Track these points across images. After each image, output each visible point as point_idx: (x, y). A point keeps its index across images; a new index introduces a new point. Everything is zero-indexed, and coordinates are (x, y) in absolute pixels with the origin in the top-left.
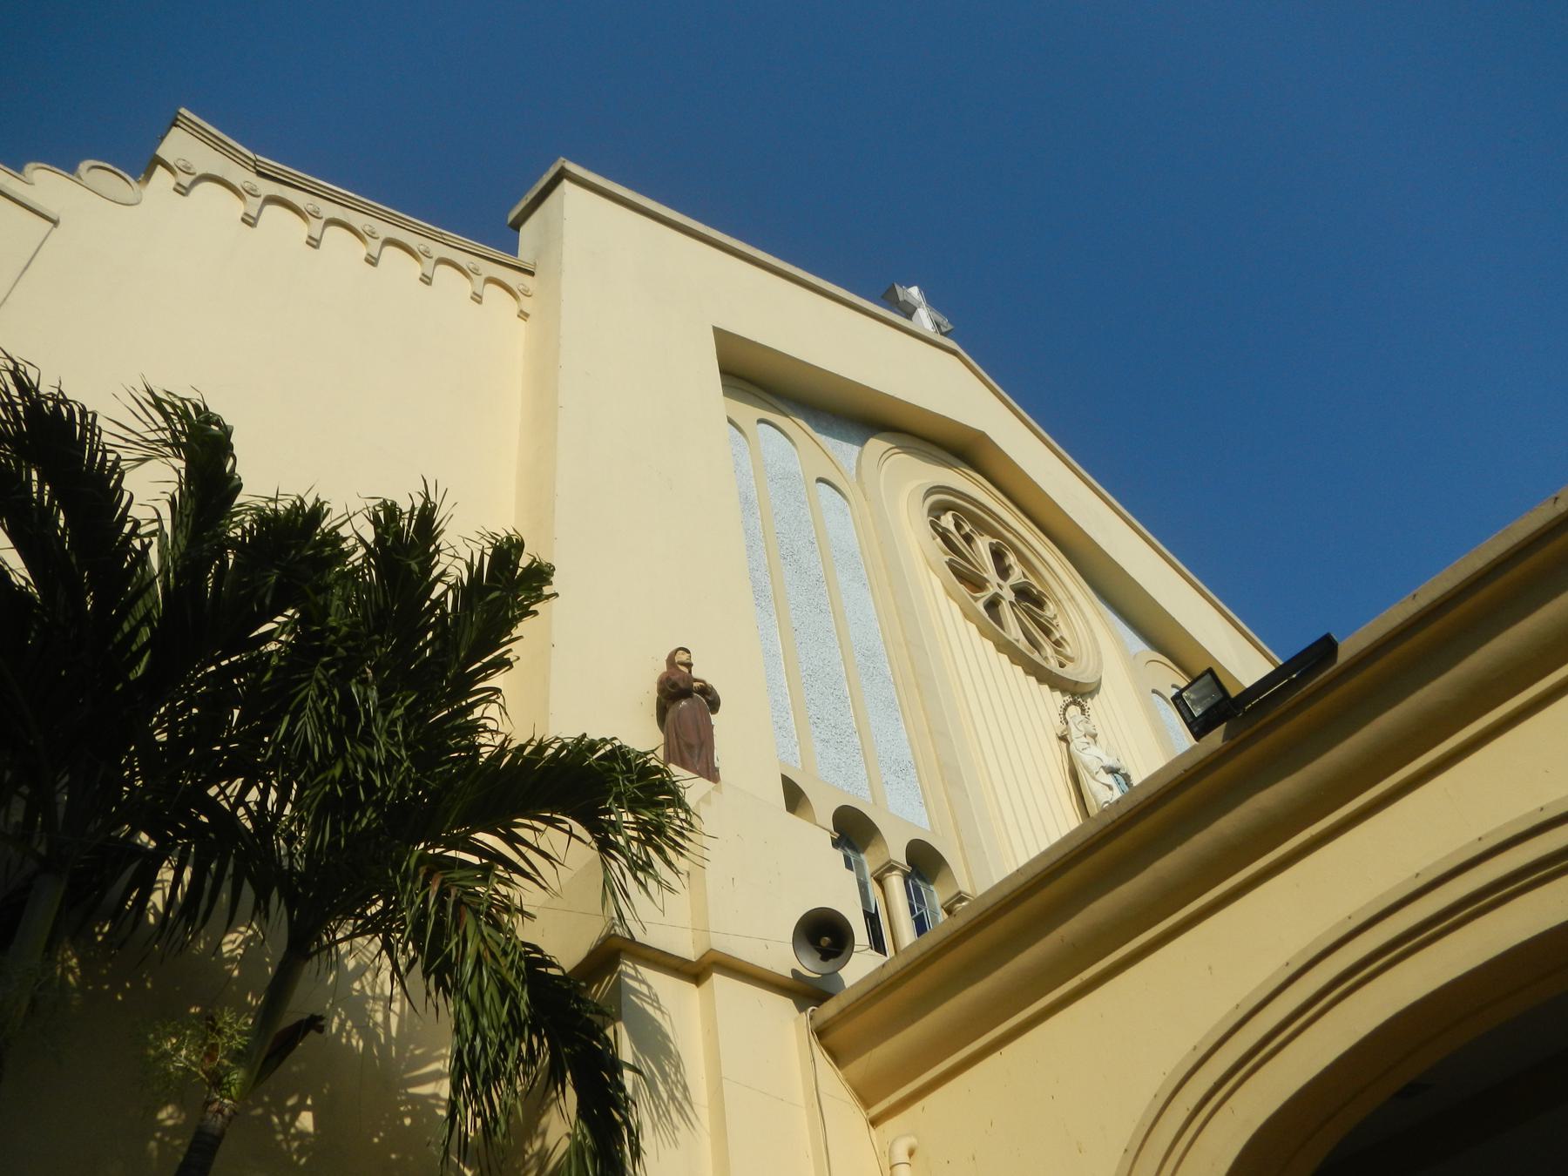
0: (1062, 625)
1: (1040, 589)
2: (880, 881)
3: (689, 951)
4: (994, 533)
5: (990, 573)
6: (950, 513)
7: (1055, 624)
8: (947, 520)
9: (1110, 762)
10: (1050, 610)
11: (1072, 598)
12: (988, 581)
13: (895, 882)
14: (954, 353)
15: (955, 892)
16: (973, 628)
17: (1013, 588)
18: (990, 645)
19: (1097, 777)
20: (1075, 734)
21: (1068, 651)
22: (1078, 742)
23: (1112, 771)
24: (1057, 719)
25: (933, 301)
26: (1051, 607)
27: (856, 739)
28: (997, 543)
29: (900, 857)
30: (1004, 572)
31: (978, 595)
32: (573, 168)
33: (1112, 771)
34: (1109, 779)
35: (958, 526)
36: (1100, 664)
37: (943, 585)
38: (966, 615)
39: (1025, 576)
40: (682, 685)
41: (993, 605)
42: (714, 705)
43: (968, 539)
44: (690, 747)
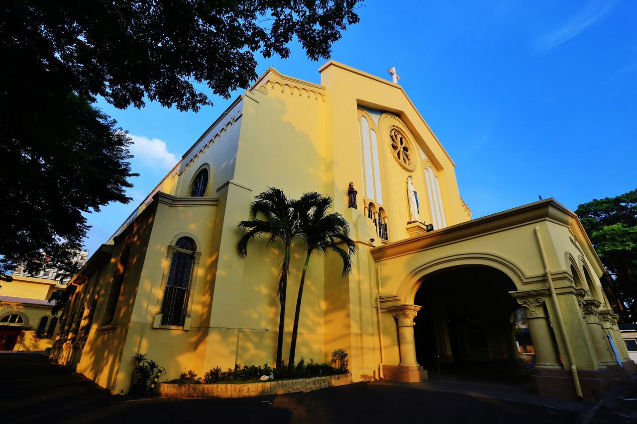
2: (374, 214)
4: (402, 135)
5: (399, 145)
8: (393, 132)
11: (414, 149)
14: (400, 89)
17: (403, 148)
21: (411, 161)
23: (414, 192)
24: (406, 179)
29: (377, 210)
30: (402, 144)
33: (414, 192)
34: (413, 193)
36: (416, 166)
41: (398, 154)
43: (396, 136)
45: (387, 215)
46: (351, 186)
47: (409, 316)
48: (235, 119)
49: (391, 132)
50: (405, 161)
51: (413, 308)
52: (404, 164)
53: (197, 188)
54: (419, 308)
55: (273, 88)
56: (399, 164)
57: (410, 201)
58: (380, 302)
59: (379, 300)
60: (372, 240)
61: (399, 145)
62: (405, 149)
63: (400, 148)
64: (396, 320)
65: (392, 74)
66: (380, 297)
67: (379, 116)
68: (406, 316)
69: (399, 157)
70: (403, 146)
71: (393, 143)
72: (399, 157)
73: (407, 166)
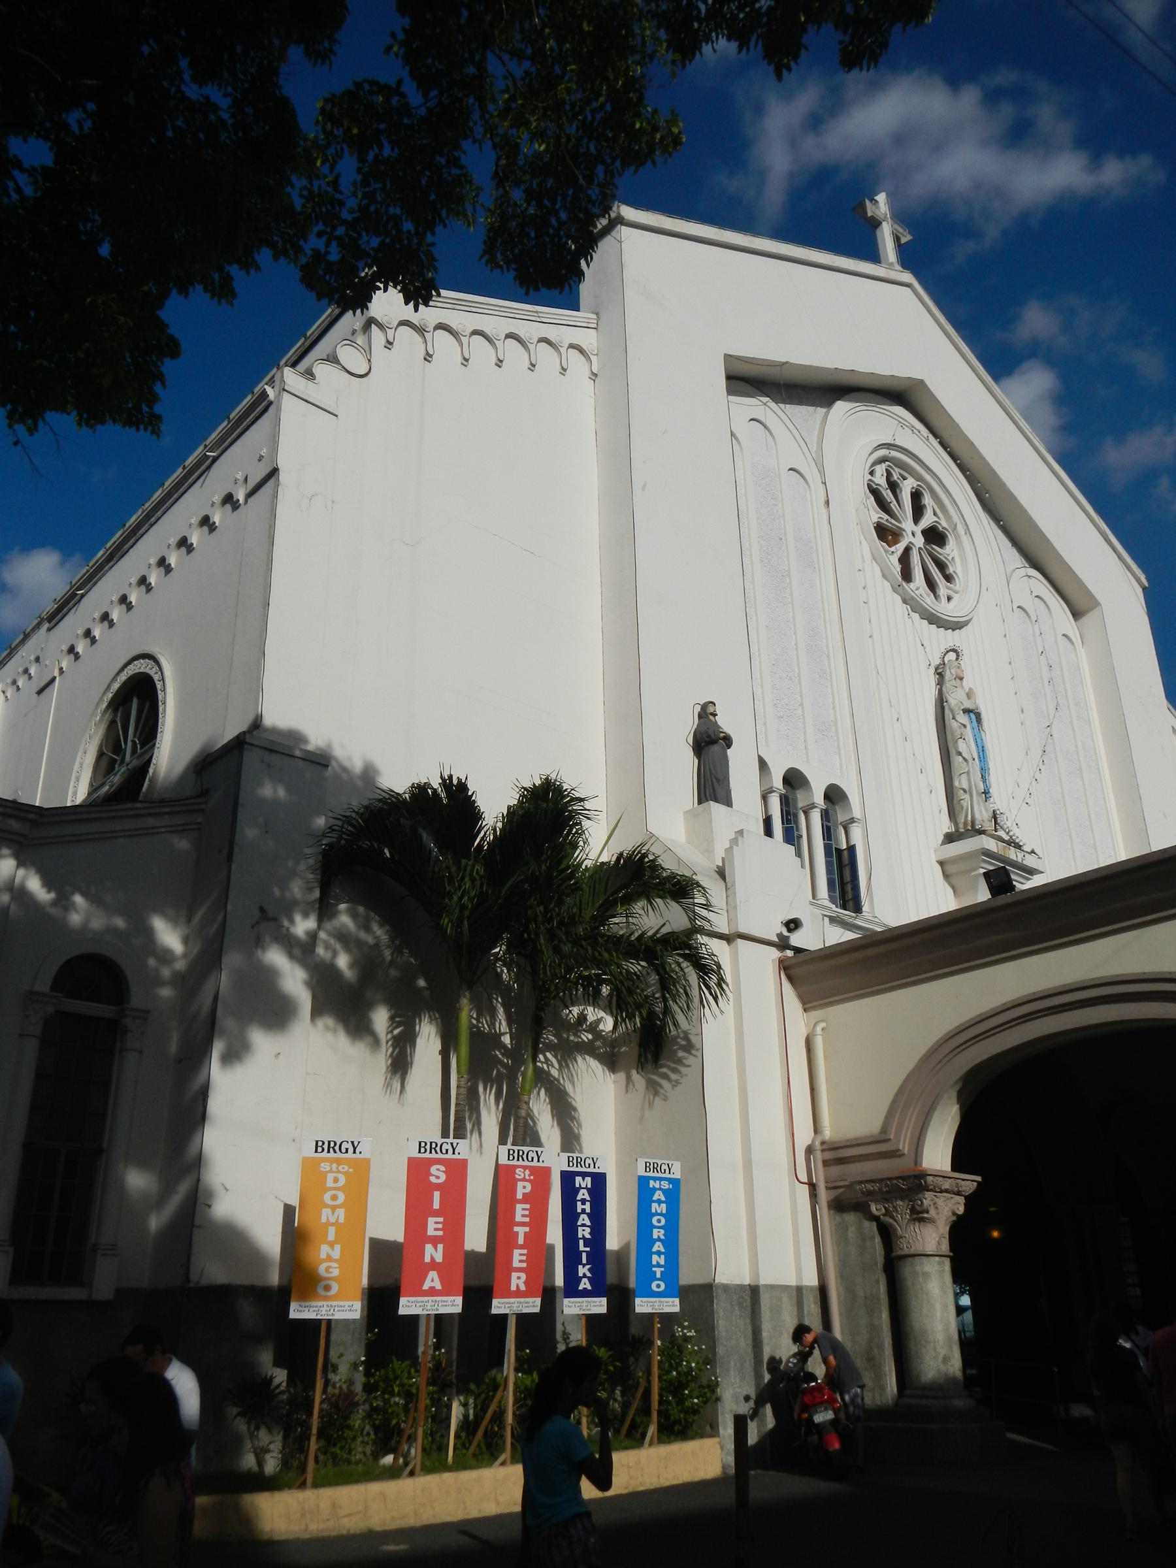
0: (957, 560)
1: (944, 524)
2: (806, 813)
3: (724, 929)
4: (919, 478)
5: (908, 524)
6: (887, 463)
7: (950, 558)
8: (880, 470)
9: (968, 705)
10: (949, 551)
11: (968, 530)
12: (904, 530)
13: (816, 816)
15: (851, 817)
16: (887, 585)
17: (924, 532)
18: (898, 599)
19: (958, 717)
20: (948, 676)
21: (958, 584)
22: (948, 687)
23: (967, 711)
25: (900, 217)
26: (951, 541)
27: (800, 711)
28: (918, 485)
29: (819, 799)
30: (918, 512)
31: (893, 549)
32: (628, 212)
33: (967, 711)
34: (963, 719)
35: (889, 474)
37: (872, 553)
38: (884, 576)
39: (935, 514)
40: (713, 737)
42: (729, 746)
43: (893, 486)
44: (718, 780)
45: (857, 813)
46: (706, 713)
47: (933, 1212)
48: (251, 484)
49: (872, 473)
50: (931, 584)
51: (946, 1185)
52: (928, 599)
53: (117, 749)
54: (970, 1182)
55: (389, 344)
56: (905, 601)
57: (953, 752)
58: (826, 1163)
59: (819, 1156)
60: (793, 925)
61: (908, 524)
62: (935, 536)
63: (912, 534)
64: (887, 1234)
65: (875, 224)
66: (823, 1143)
67: (821, 411)
68: (919, 1216)
69: (907, 575)
70: (927, 520)
71: (876, 515)
72: (907, 575)
73: (945, 609)
